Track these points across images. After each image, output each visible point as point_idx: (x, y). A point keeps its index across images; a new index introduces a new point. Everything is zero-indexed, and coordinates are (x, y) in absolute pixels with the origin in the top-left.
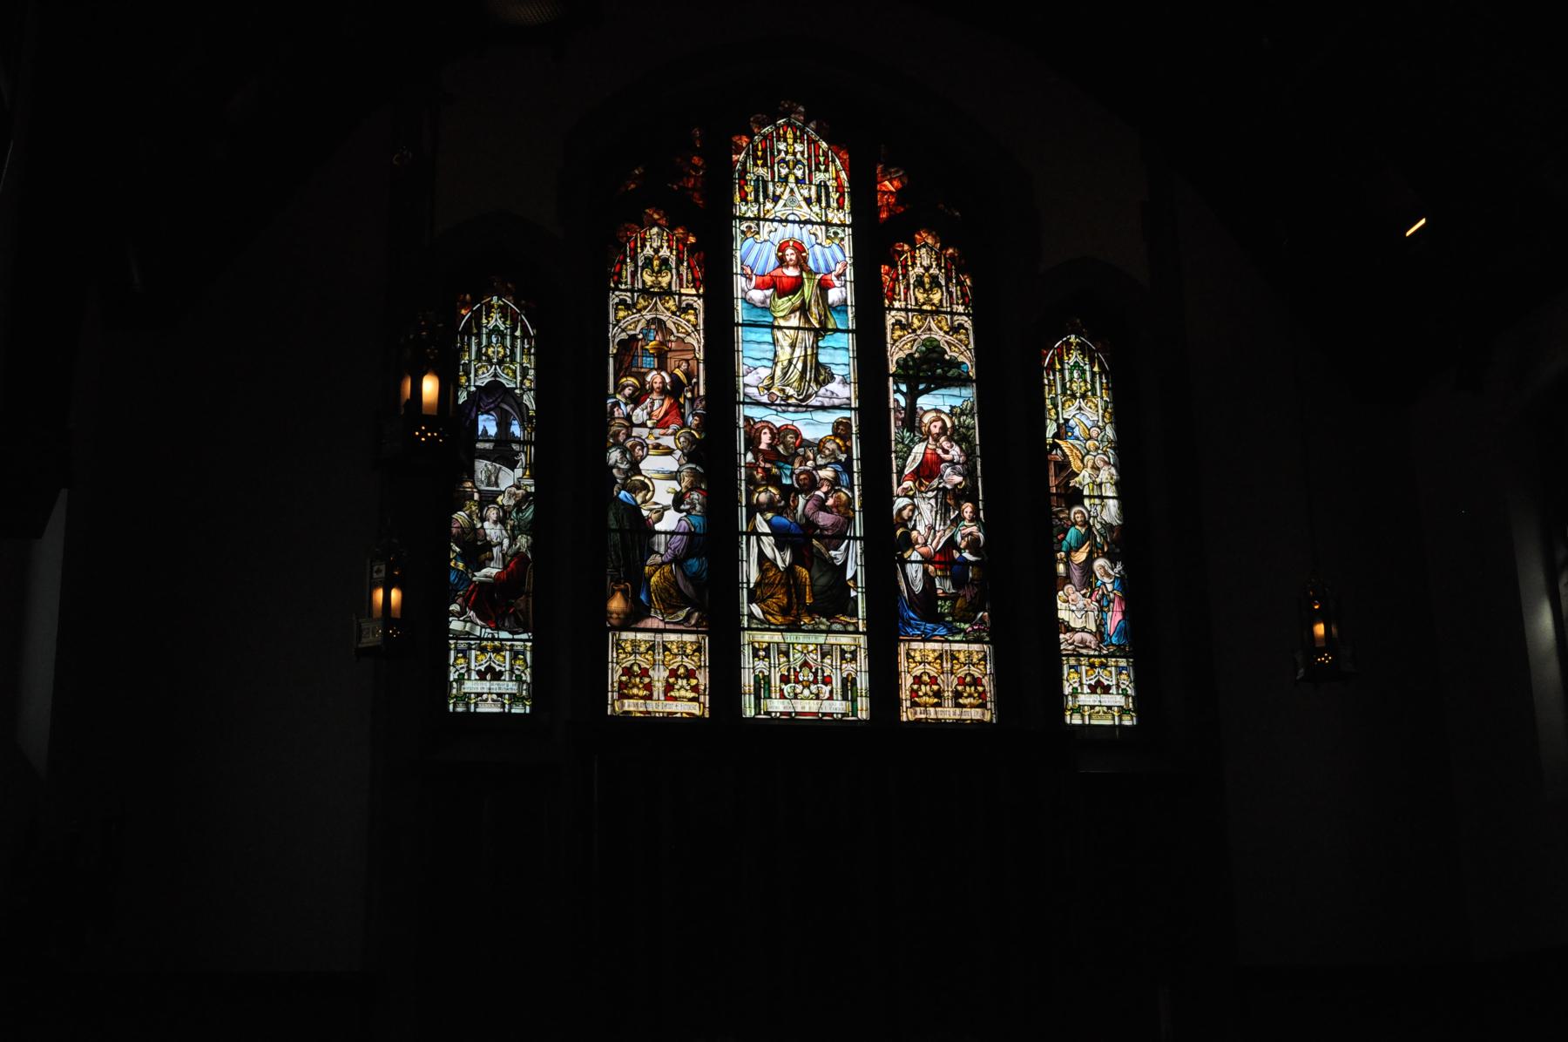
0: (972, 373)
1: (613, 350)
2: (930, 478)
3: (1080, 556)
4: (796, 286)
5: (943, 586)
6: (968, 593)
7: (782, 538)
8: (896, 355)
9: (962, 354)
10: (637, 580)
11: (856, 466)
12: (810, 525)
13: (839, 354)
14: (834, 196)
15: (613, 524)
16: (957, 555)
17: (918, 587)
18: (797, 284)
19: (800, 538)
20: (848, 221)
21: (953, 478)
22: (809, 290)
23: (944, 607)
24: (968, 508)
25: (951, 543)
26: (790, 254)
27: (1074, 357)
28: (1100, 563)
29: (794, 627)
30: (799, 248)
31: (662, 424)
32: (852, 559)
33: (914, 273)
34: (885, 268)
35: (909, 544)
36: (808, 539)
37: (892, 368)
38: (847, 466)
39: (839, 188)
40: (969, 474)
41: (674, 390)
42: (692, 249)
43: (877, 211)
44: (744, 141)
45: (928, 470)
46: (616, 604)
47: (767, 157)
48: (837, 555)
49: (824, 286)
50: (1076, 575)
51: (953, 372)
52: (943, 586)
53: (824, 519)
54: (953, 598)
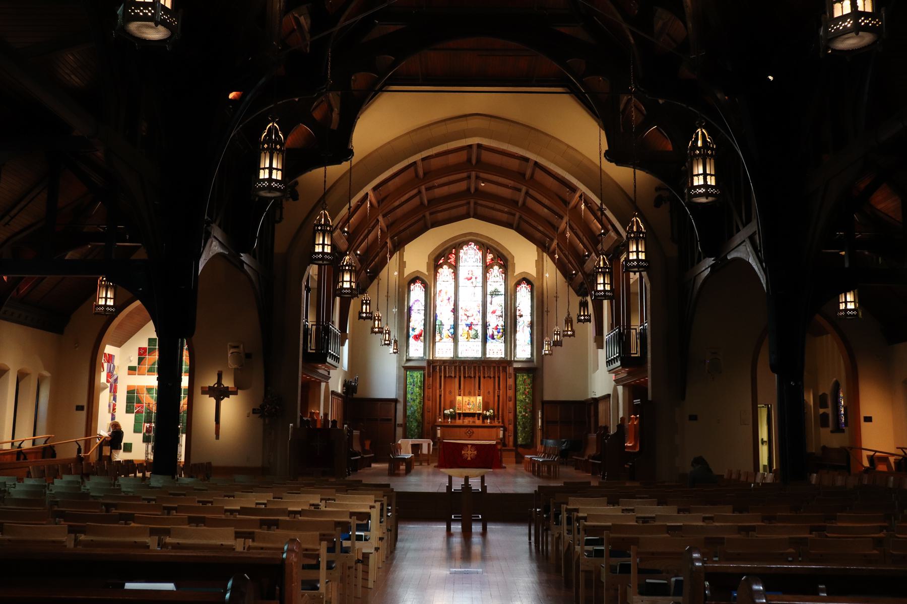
0: (504, 294)
1: (438, 292)
2: (494, 313)
3: (521, 327)
4: (471, 278)
5: (496, 333)
6: (500, 334)
7: (467, 325)
8: (490, 289)
9: (502, 289)
10: (440, 333)
11: (481, 312)
12: (472, 323)
13: (479, 291)
14: (479, 260)
15: (437, 324)
16: (498, 327)
17: (491, 334)
18: (471, 278)
19: (470, 326)
20: (481, 265)
21: (499, 313)
22: (474, 278)
23: (495, 337)
24: (501, 318)
25: (498, 325)
26: (470, 273)
27: (524, 287)
28: (526, 327)
29: (468, 341)
30: (472, 271)
31: (446, 305)
32: (479, 328)
33: (493, 275)
34: (488, 274)
35: (489, 325)
36: (471, 325)
37: (488, 293)
38: (479, 312)
39: (480, 259)
40: (502, 312)
41: (449, 299)
42: (453, 273)
43: (487, 263)
44: (461, 251)
45: (494, 312)
46: (438, 338)
47: (465, 254)
48: (476, 328)
49: (476, 278)
50: (521, 330)
51: (500, 293)
52: (496, 333)
53: (475, 322)
54: (497, 335)
